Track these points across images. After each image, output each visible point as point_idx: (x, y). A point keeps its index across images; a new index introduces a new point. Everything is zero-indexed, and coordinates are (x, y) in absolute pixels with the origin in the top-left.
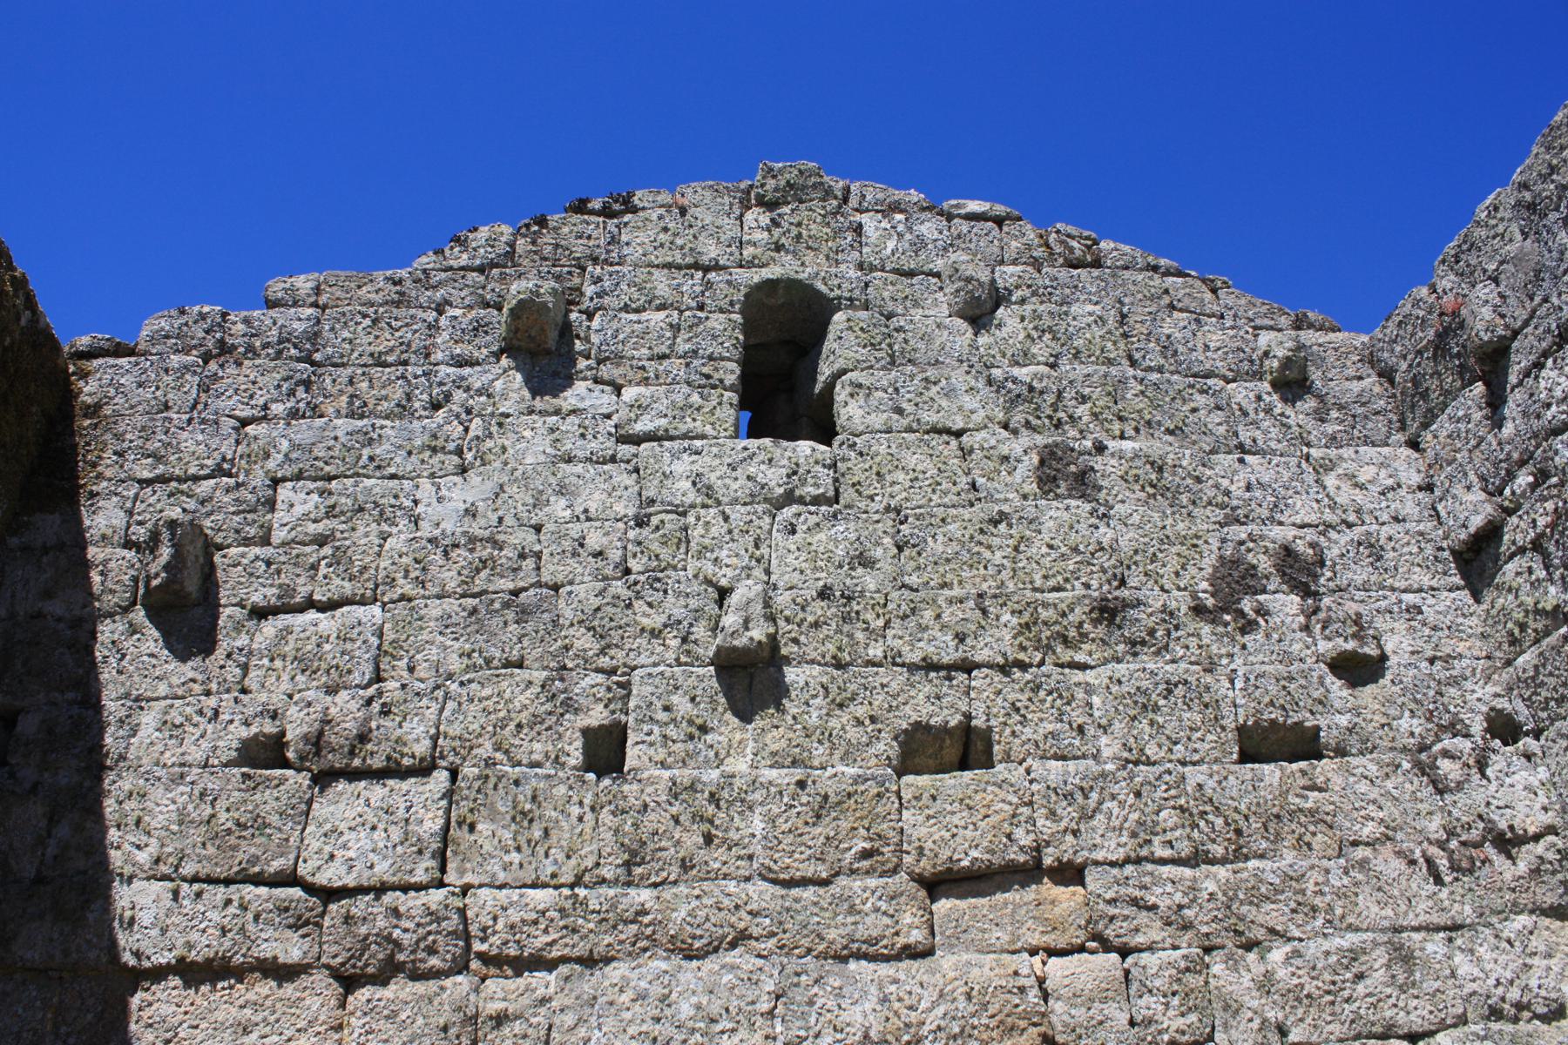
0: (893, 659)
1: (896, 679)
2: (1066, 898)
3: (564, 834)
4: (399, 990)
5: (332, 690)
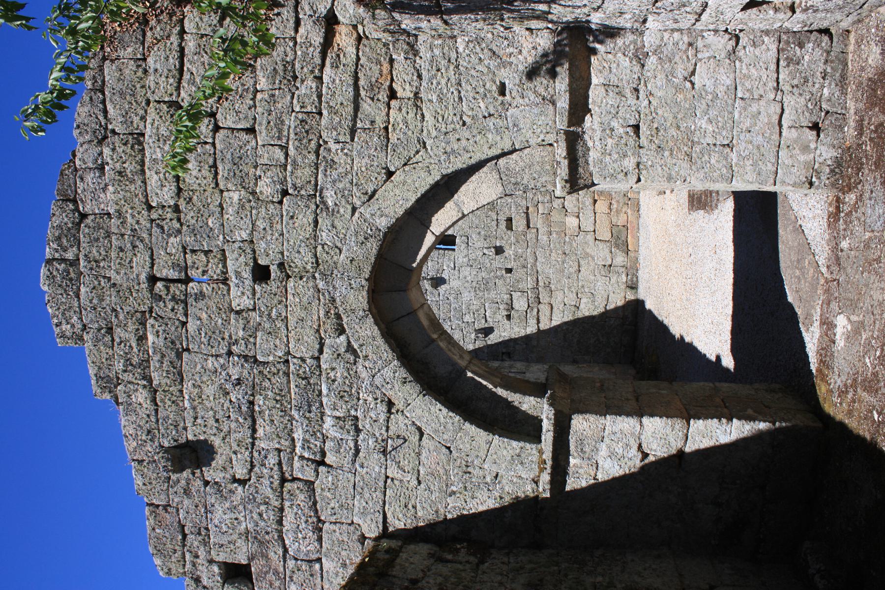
0: (496, 231)
1: (499, 230)
2: (531, 209)
3: (521, 276)
4: (540, 296)
5: (499, 309)
